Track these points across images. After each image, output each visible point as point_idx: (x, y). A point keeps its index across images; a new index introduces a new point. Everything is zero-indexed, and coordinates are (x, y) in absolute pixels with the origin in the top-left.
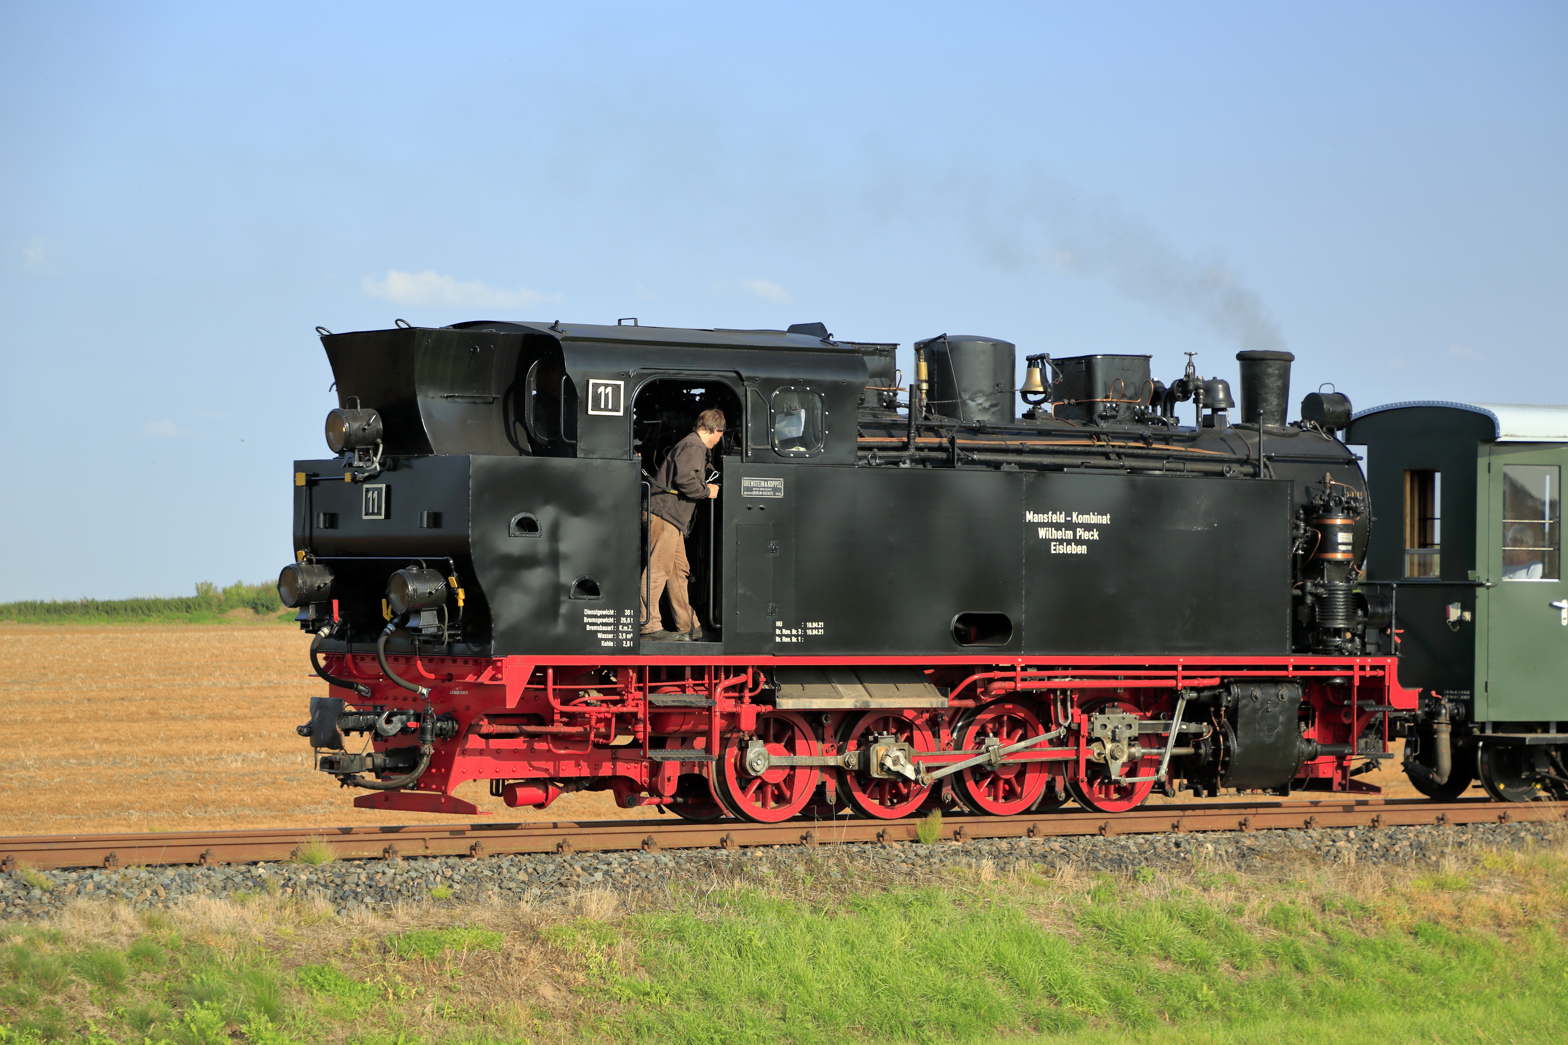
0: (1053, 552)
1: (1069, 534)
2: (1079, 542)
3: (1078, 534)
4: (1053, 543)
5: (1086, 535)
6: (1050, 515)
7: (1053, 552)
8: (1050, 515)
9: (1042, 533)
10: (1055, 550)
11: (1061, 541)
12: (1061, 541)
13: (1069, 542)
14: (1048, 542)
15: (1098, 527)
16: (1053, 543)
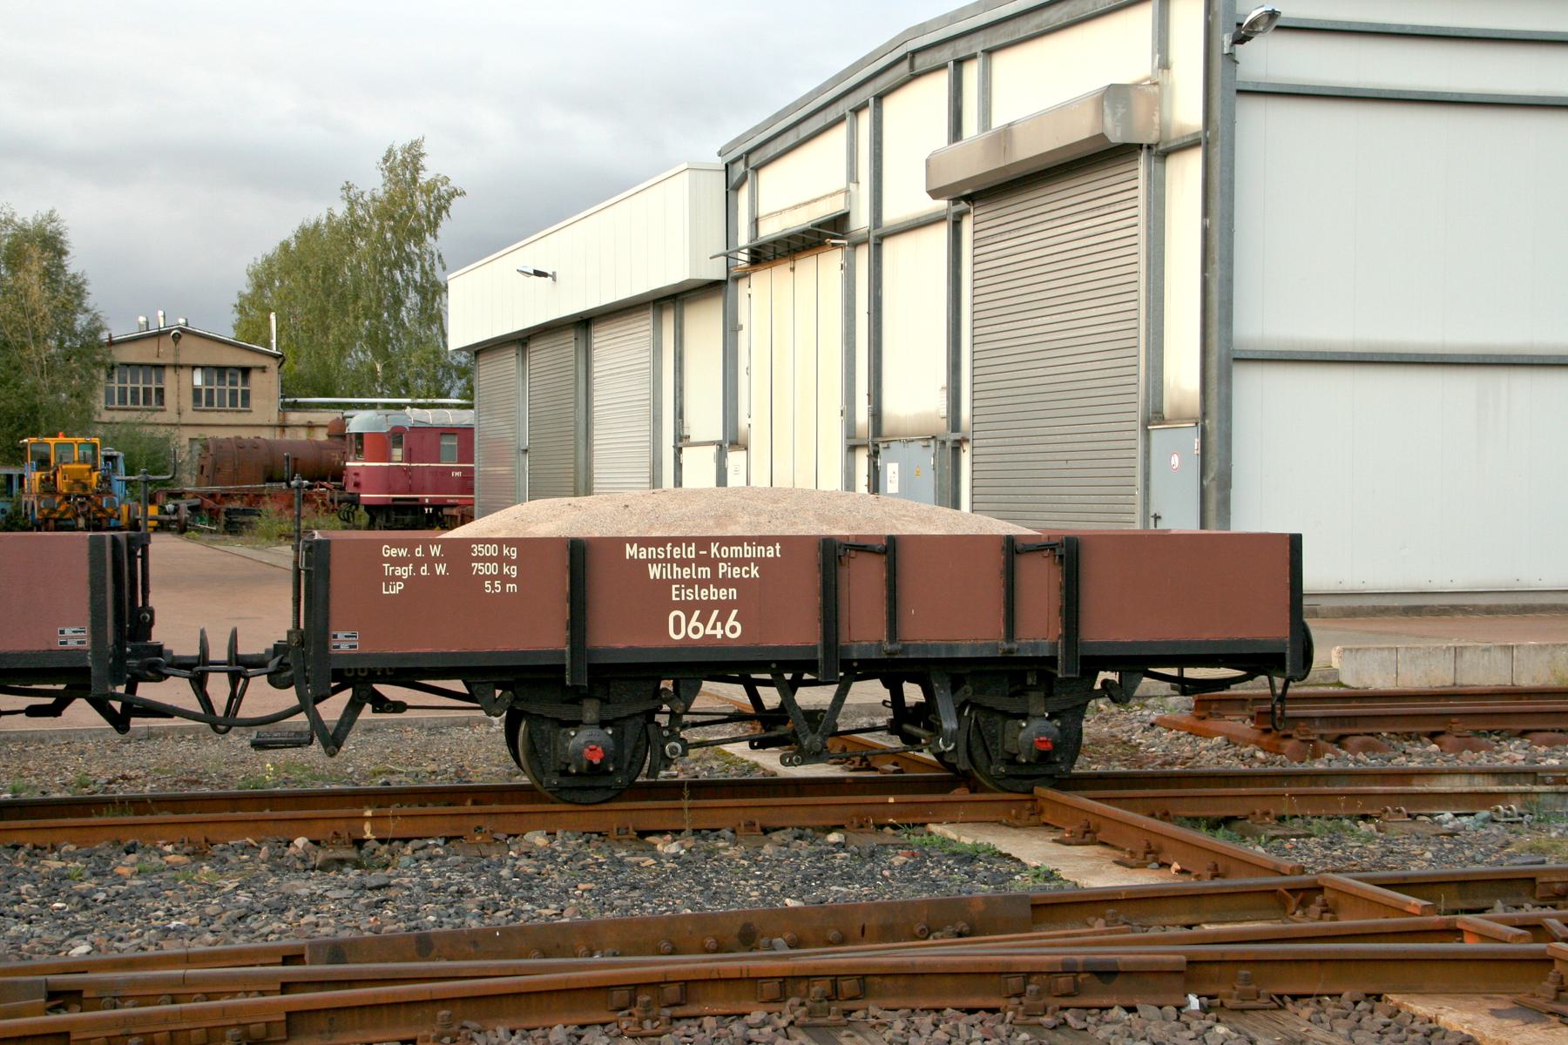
0: (674, 598)
1: (705, 572)
2: (726, 583)
3: (721, 571)
4: (674, 587)
5: (736, 572)
6: (669, 548)
7: (674, 598)
8: (669, 548)
9: (654, 571)
10: (677, 596)
11: (689, 583)
12: (689, 583)
13: (704, 584)
14: (665, 584)
15: (759, 561)
16: (674, 587)
